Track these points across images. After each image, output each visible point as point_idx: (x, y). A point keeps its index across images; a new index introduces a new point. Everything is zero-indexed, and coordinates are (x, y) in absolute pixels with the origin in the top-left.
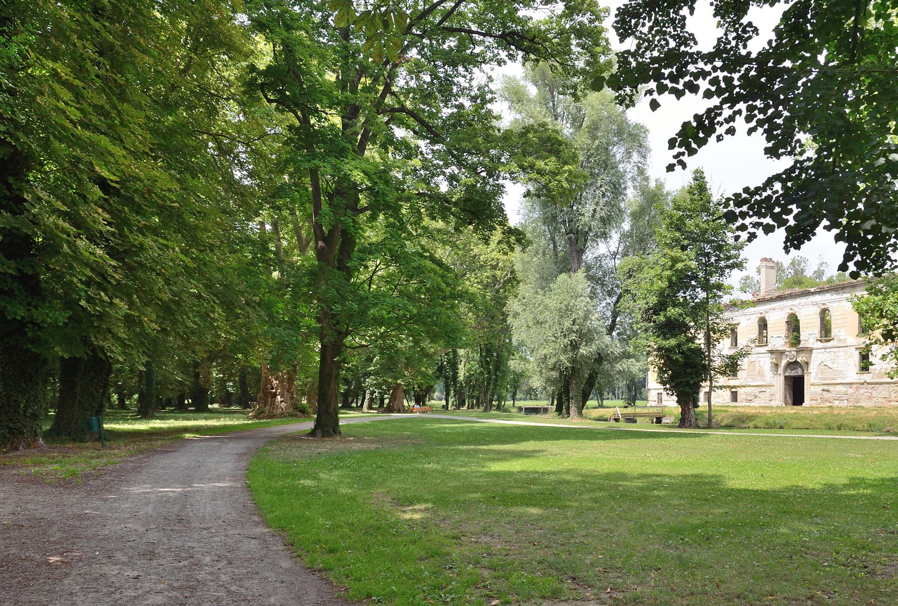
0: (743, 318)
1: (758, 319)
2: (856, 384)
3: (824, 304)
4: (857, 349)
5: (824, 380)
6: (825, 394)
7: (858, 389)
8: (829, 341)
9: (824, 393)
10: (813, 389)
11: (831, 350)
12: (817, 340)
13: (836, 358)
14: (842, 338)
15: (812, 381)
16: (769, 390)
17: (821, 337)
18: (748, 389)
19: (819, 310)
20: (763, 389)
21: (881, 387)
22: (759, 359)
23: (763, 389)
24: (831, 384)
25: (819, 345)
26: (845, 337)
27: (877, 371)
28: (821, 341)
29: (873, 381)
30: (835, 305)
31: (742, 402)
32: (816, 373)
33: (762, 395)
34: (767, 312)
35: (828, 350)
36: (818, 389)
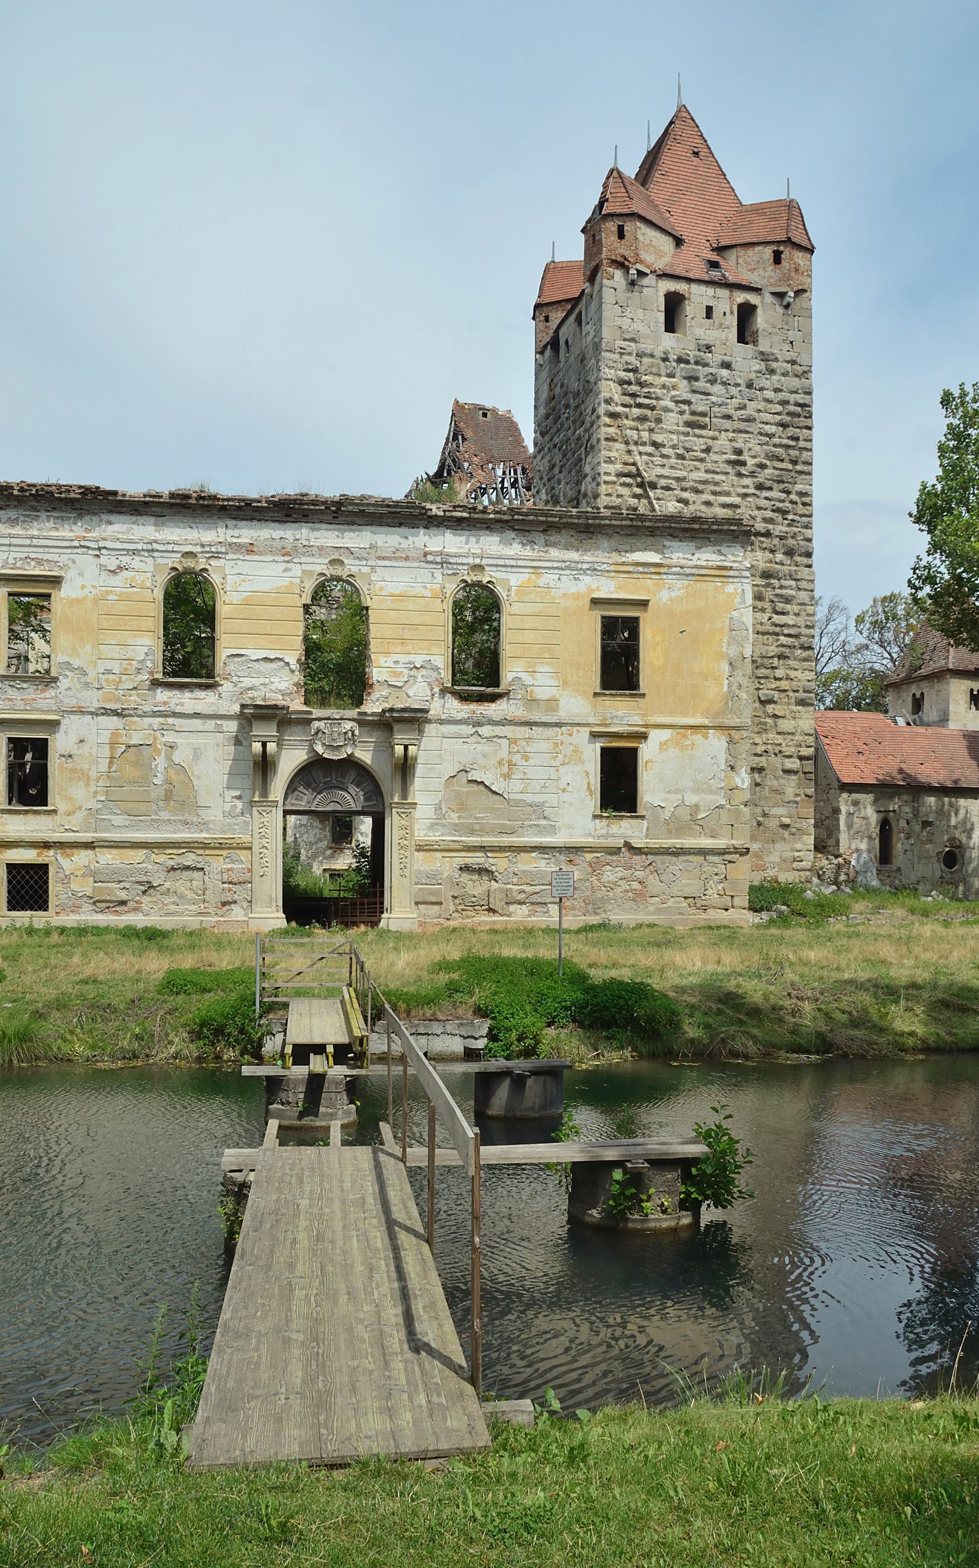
0: (87, 561)
1: (163, 578)
2: (592, 849)
3: (479, 568)
4: (595, 736)
5: (472, 832)
6: (476, 887)
7: (595, 867)
8: (493, 698)
9: (465, 877)
10: (421, 862)
11: (499, 730)
12: (444, 691)
13: (516, 758)
14: (542, 694)
15: (421, 833)
16: (217, 864)
17: (454, 682)
18: (107, 858)
19: (452, 587)
20: (190, 859)
21: (676, 865)
22: (170, 737)
23: (190, 859)
24: (501, 849)
25: (455, 707)
26: (554, 692)
27: (667, 815)
28: (454, 693)
29: (654, 843)
30: (515, 579)
31: (75, 909)
32: (438, 807)
33: (181, 883)
34: (216, 556)
35: (486, 730)
36: (447, 865)
